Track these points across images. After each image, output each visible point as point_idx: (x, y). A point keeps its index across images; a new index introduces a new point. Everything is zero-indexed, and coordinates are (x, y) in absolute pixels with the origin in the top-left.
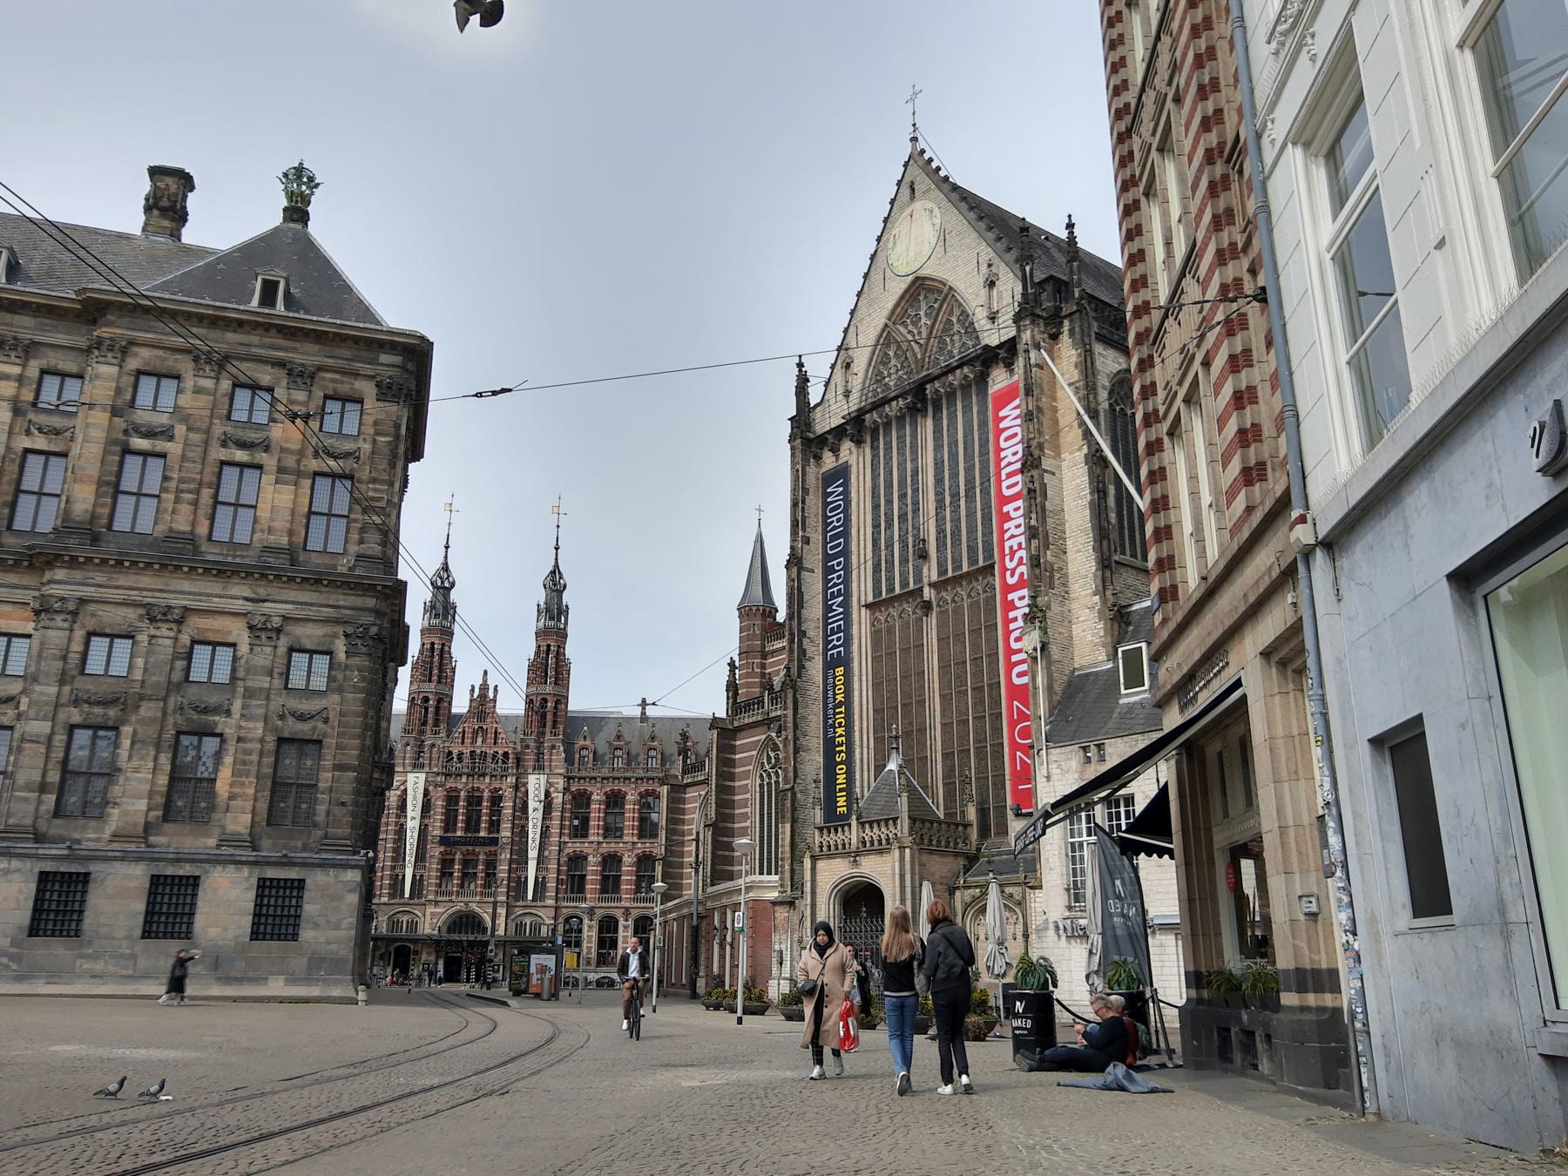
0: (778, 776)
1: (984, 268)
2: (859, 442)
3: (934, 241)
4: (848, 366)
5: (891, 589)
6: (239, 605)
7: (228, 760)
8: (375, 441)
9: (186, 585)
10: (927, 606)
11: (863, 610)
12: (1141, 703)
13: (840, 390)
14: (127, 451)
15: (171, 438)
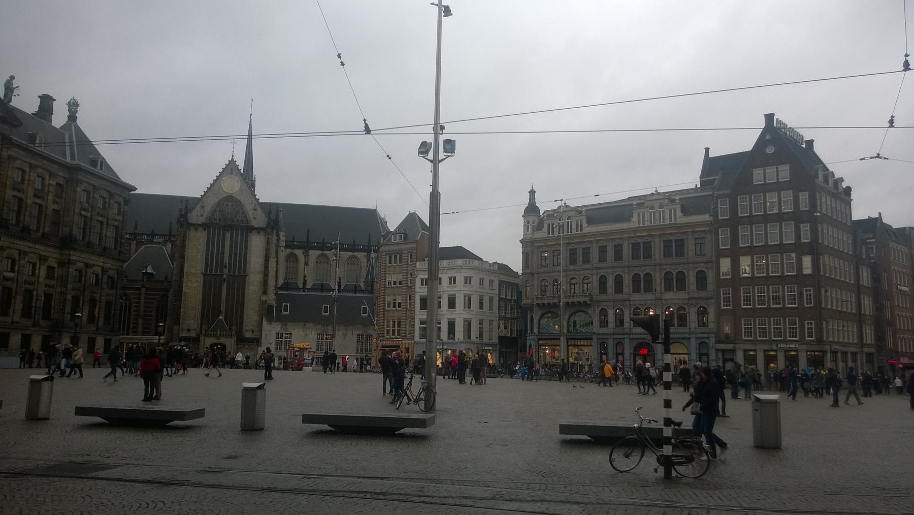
0: (126, 303)
1: (253, 205)
2: (205, 230)
3: (237, 190)
4: (203, 207)
5: (211, 270)
6: (101, 264)
7: (98, 307)
8: (123, 218)
9: (93, 258)
10: (225, 280)
11: (202, 275)
12: (286, 315)
13: (199, 214)
14: (81, 215)
15: (88, 212)
